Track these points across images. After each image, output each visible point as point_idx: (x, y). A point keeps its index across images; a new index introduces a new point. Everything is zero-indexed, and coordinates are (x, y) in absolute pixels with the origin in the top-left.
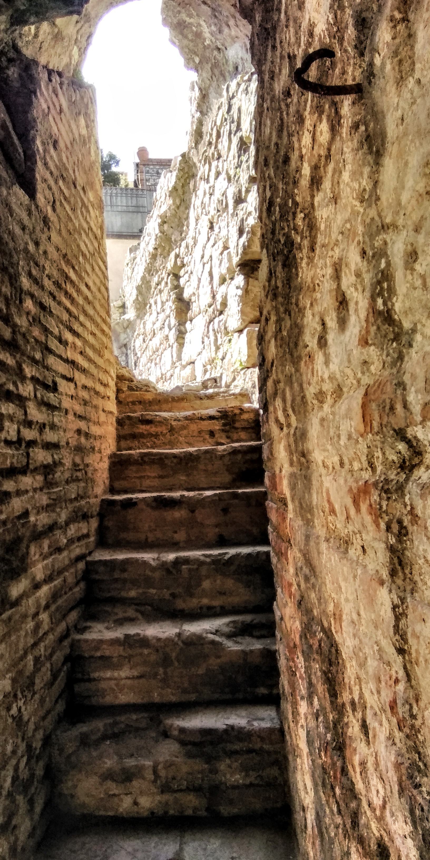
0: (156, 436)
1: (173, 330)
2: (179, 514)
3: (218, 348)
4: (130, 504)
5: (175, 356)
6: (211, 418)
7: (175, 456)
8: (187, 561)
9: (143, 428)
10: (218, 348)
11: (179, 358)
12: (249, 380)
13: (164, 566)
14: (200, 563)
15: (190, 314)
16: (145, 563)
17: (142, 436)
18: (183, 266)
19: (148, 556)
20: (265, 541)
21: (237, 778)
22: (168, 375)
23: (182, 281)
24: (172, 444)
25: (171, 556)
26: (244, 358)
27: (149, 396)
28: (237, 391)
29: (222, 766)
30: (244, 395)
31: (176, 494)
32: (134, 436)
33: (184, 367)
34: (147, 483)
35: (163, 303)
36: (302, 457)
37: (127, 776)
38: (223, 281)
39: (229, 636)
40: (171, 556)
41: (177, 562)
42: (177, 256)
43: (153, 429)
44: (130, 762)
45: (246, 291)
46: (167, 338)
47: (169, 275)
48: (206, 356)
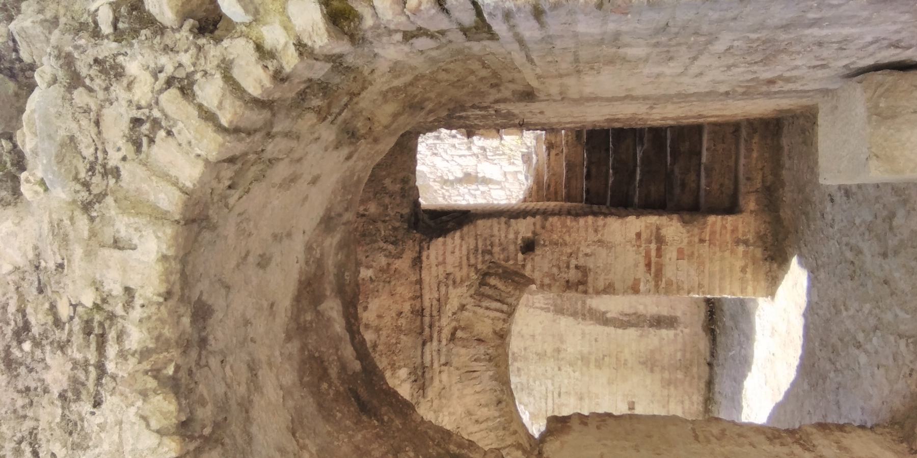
0: (556, 183)
1: (480, 187)
2: (594, 170)
3: (504, 154)
4: (588, 191)
5: (497, 187)
6: (549, 155)
7: (567, 172)
8: (613, 165)
9: (552, 189)
10: (504, 154)
11: (498, 183)
12: (529, 137)
13: (615, 174)
14: (614, 159)
15: (473, 174)
16: (613, 182)
17: (556, 189)
18: (442, 177)
19: (610, 182)
20: (608, 130)
21: (687, 144)
22: (508, 193)
23: (451, 178)
24: (561, 176)
25: (611, 171)
26: (517, 137)
27: (535, 187)
28: (534, 142)
29: (682, 149)
30: (537, 139)
31: (585, 170)
32: (556, 193)
33: (507, 179)
34: (579, 185)
35: (459, 195)
36: (569, 123)
37: (683, 185)
38: (469, 148)
39: (643, 145)
40: (611, 171)
41: (613, 169)
42: (435, 181)
43: (553, 184)
44: (679, 182)
45: (482, 135)
46: (483, 193)
47: (442, 188)
48: (505, 163)
